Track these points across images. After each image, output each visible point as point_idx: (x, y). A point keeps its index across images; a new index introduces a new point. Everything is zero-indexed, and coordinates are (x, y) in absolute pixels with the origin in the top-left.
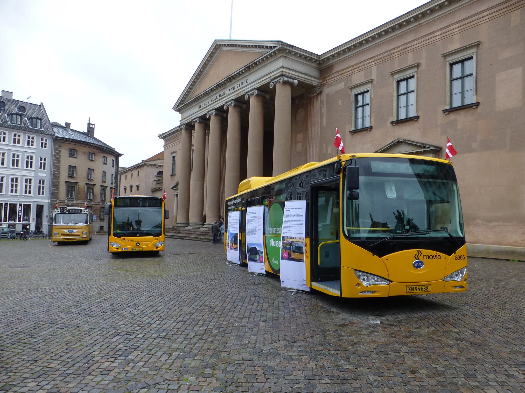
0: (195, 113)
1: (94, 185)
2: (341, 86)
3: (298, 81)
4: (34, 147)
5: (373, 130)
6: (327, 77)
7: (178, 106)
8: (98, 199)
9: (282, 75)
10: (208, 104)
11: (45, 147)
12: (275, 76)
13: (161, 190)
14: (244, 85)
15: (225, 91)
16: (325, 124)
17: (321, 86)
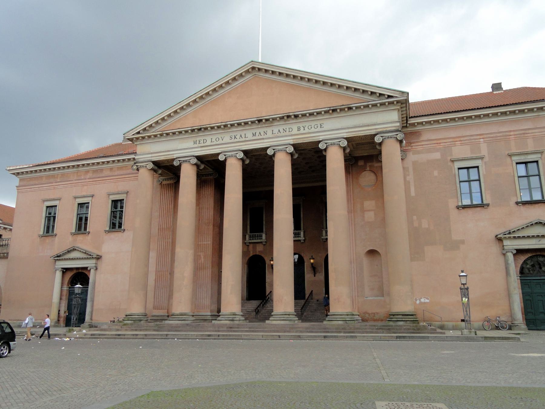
2: (437, 156)
5: (490, 207)
6: (414, 143)
7: (139, 133)
10: (221, 142)
12: (385, 130)
13: (7, 258)
14: (313, 130)
15: (269, 131)
16: (413, 193)
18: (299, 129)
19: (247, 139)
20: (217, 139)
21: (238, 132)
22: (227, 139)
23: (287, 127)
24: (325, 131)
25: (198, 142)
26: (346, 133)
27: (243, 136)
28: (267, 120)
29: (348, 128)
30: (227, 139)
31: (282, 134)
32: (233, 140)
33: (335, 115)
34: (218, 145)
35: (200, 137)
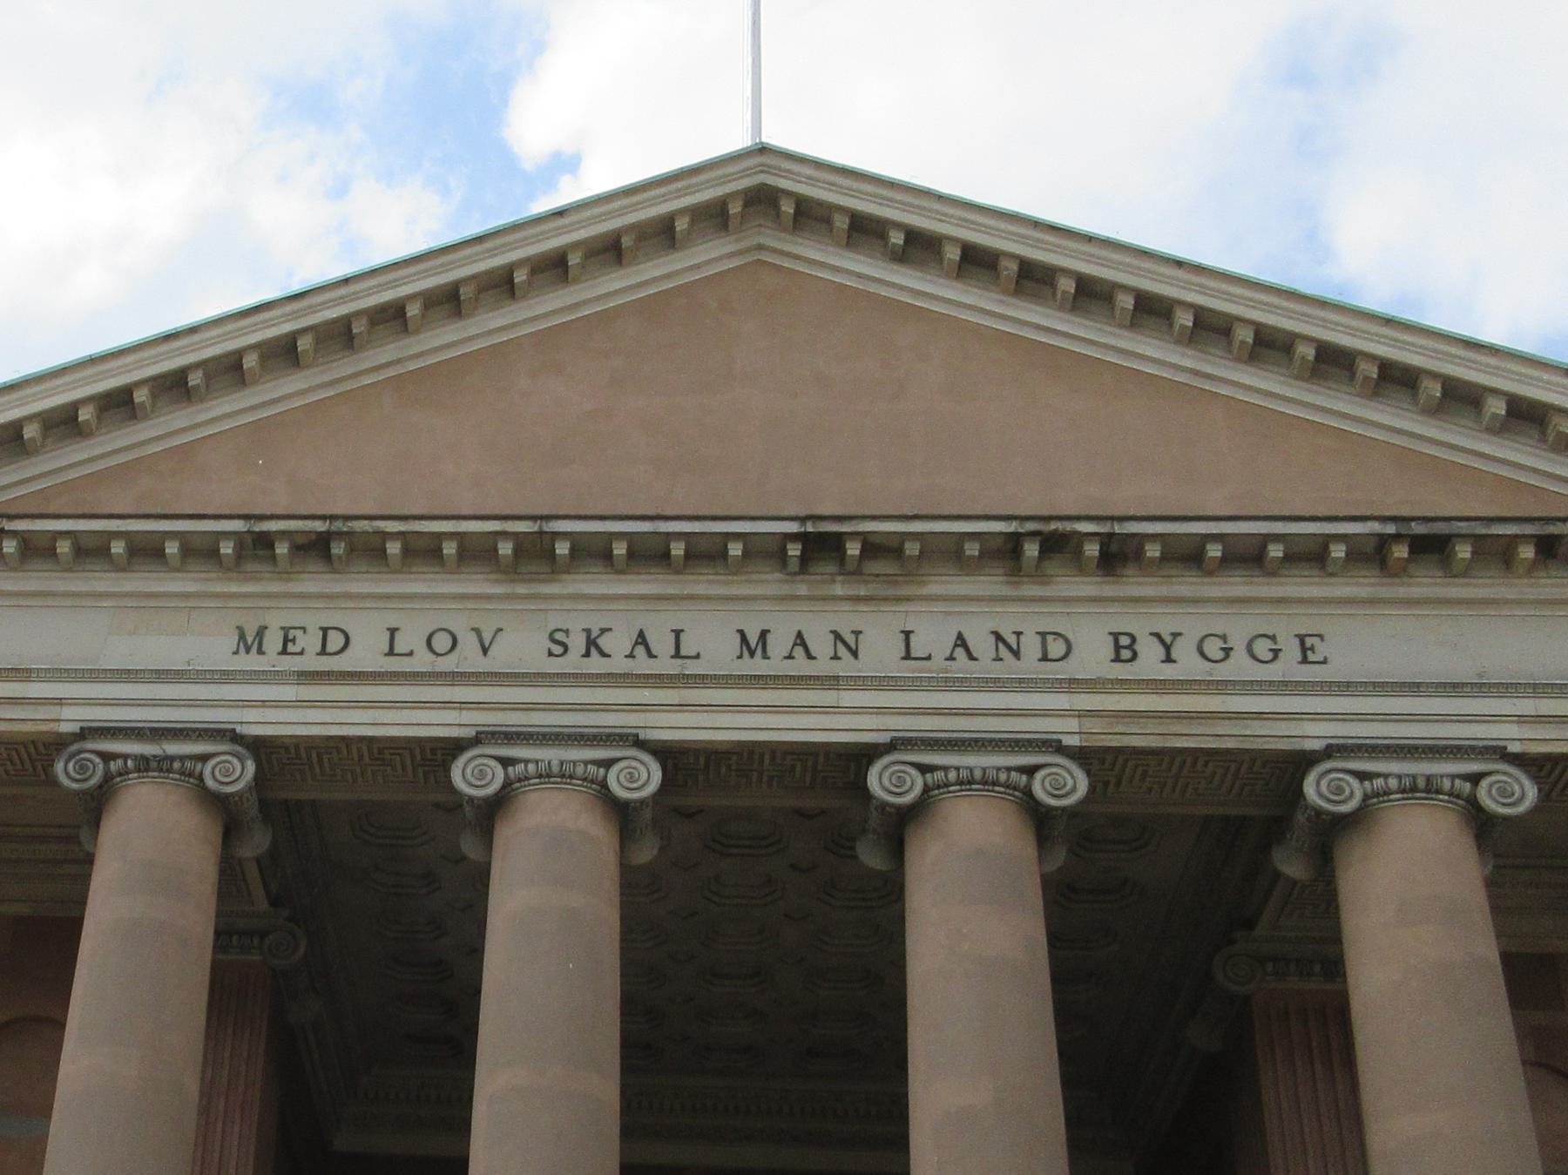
10: (469, 658)
14: (1240, 667)
18: (1124, 648)
19: (693, 668)
20: (442, 642)
21: (614, 606)
22: (521, 646)
23: (1025, 621)
24: (1346, 688)
25: (273, 642)
26: (1521, 719)
27: (662, 643)
28: (875, 548)
29: (1538, 689)
30: (521, 646)
31: (986, 666)
32: (573, 662)
33: (1426, 583)
34: (454, 678)
35: (303, 602)
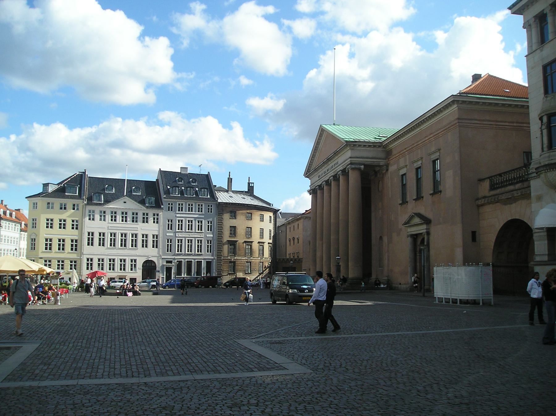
0: (327, 172)
1: (252, 242)
3: (365, 165)
4: (203, 213)
8: (256, 254)
9: (351, 164)
11: (211, 212)
17: (387, 166)
